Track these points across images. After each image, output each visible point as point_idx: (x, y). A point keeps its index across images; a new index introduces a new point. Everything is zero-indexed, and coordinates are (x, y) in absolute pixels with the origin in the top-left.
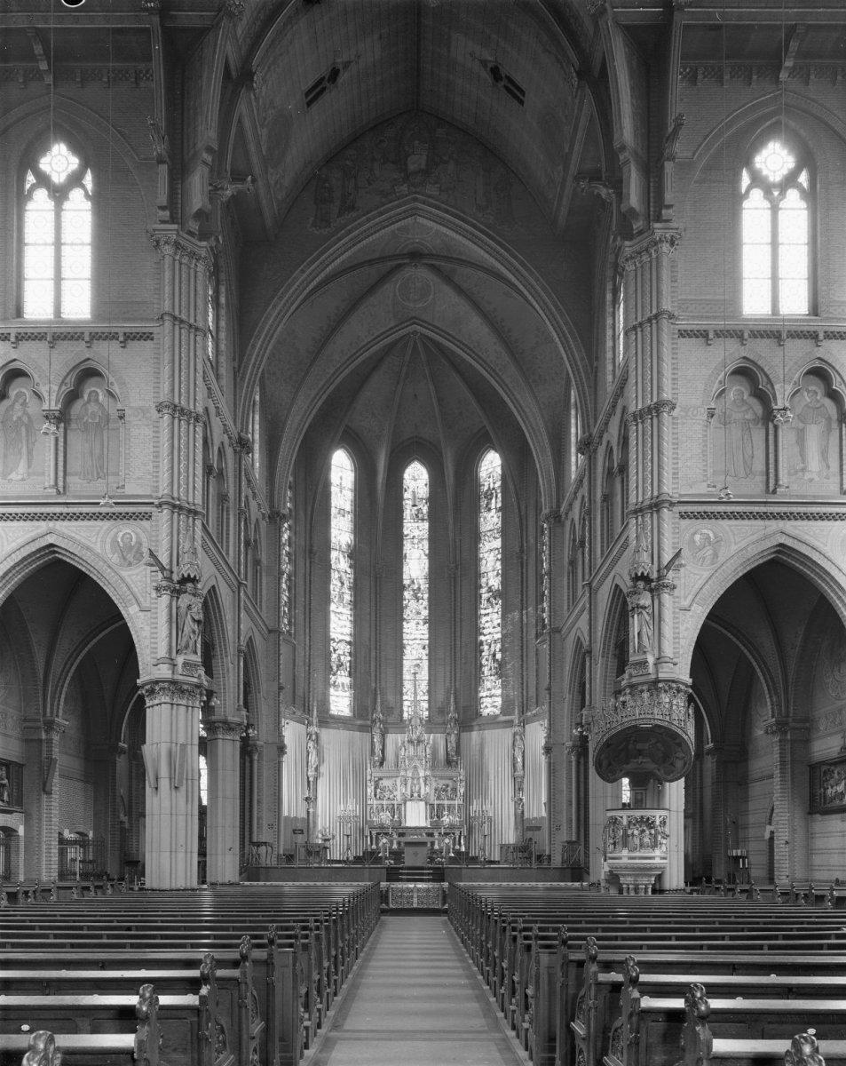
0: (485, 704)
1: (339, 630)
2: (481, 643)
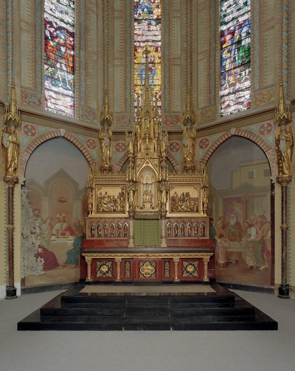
0: (227, 103)
1: (58, 14)
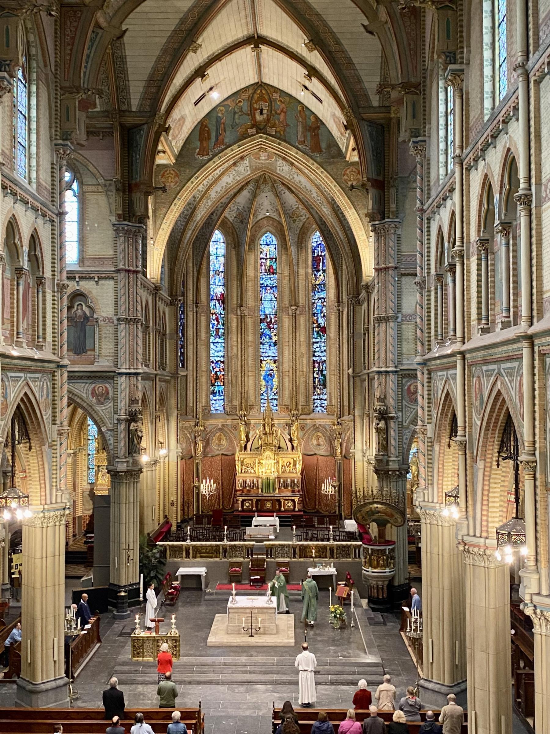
1: (216, 354)
2: (314, 361)
